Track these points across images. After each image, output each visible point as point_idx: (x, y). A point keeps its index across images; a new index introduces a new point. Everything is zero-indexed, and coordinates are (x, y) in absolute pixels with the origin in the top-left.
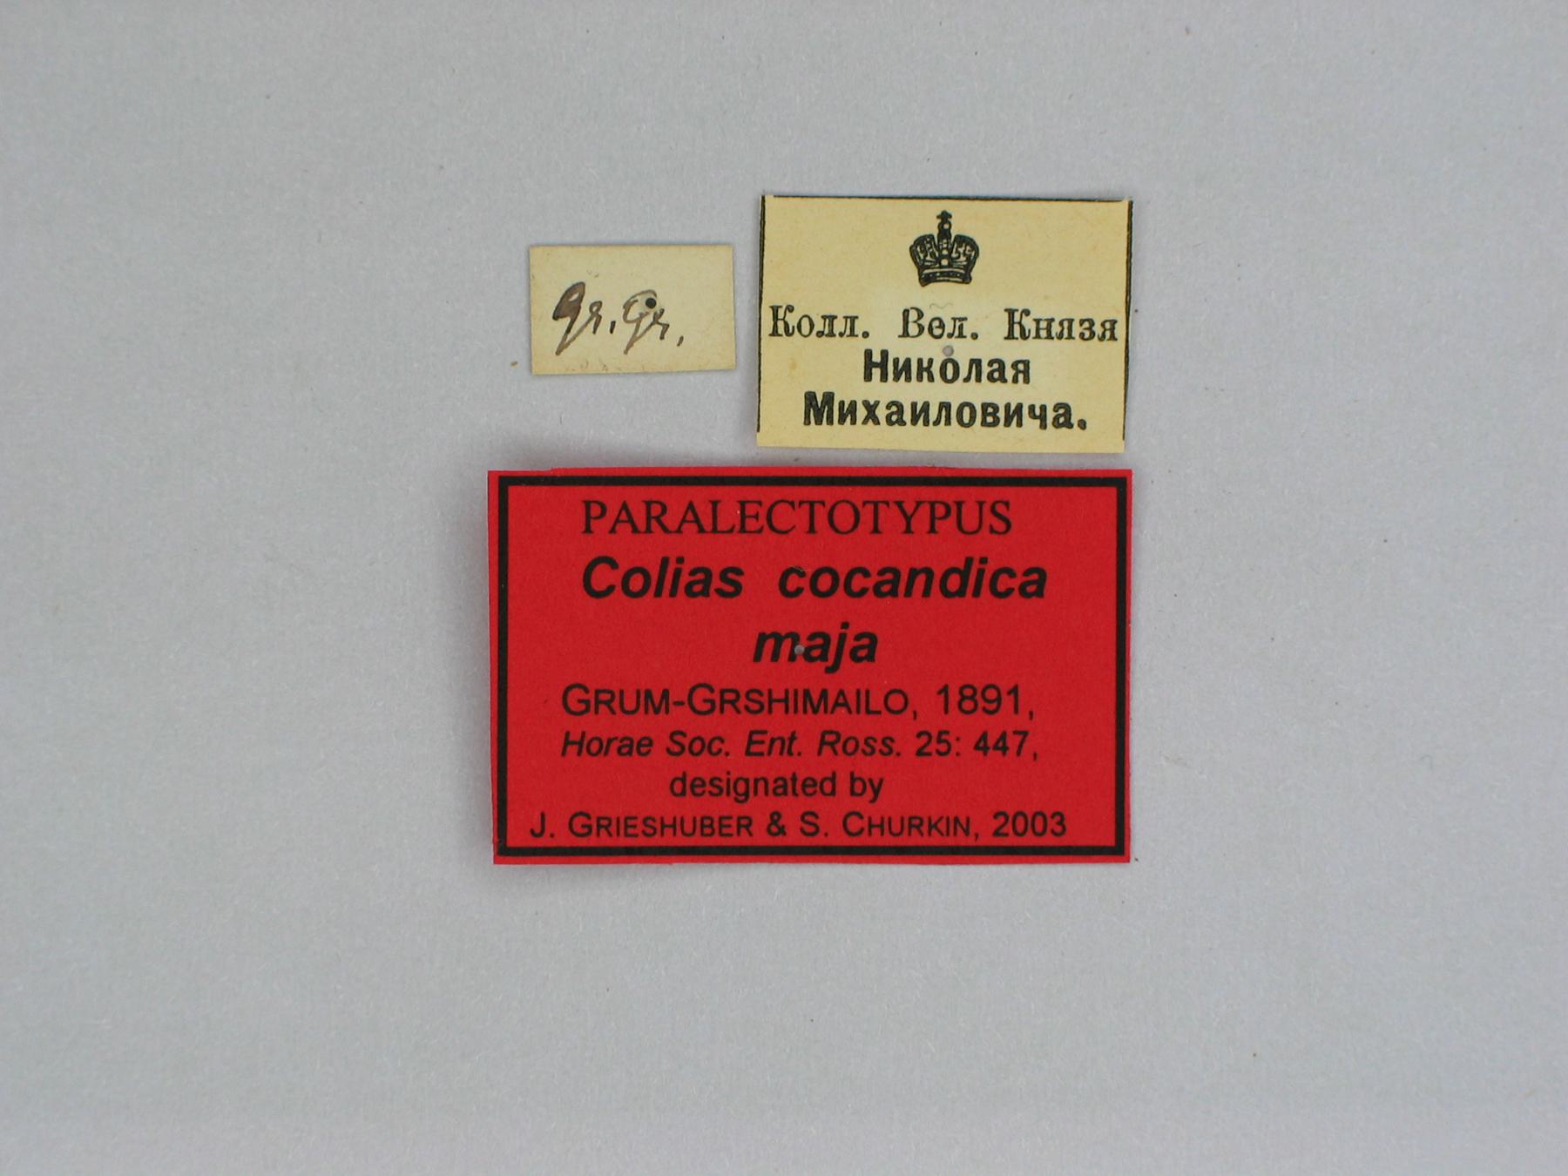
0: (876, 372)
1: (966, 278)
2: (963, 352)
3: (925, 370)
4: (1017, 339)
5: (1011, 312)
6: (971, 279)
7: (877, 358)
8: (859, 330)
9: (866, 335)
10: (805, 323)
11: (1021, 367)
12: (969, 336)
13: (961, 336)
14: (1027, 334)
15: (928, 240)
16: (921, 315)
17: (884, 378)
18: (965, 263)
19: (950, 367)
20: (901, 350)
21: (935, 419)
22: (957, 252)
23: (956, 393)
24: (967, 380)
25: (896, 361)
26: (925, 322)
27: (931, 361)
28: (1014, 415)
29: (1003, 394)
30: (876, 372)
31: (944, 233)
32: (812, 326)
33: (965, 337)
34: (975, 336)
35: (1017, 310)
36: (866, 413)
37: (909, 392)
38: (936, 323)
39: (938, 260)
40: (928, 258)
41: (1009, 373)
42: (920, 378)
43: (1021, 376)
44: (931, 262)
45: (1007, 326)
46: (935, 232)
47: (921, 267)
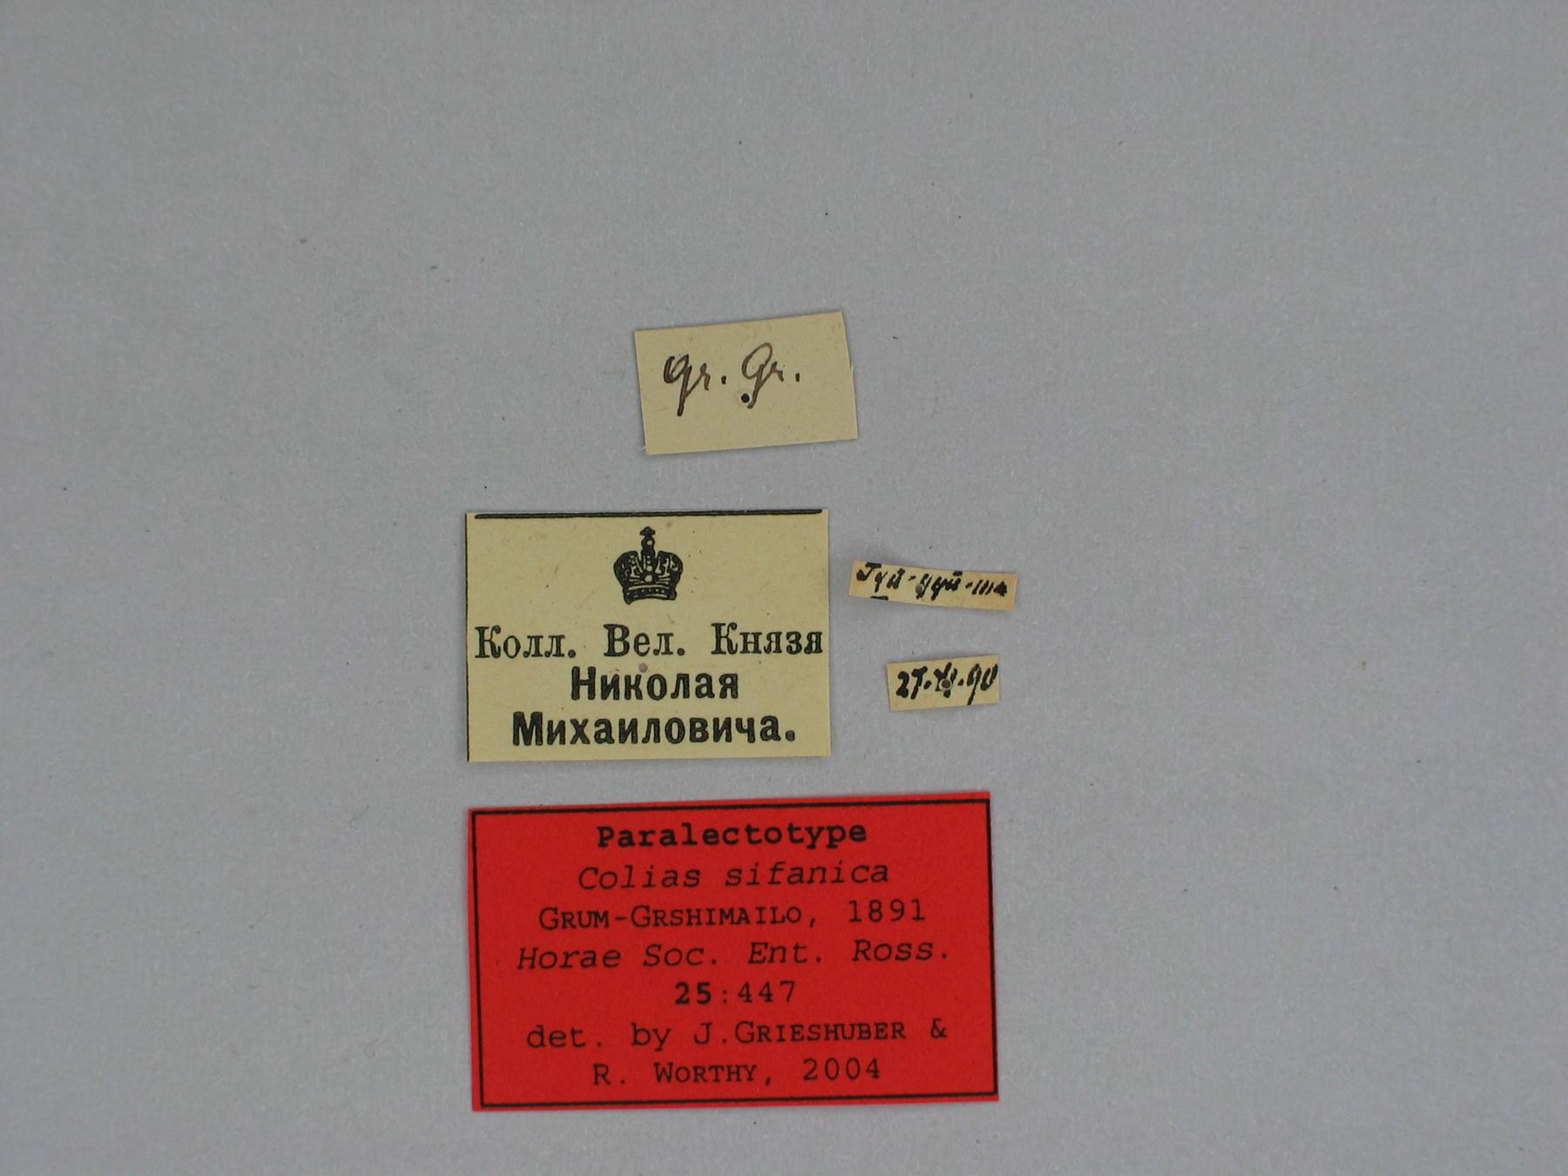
0: (584, 690)
1: (671, 593)
2: (669, 668)
3: (632, 687)
4: (725, 653)
5: (718, 627)
6: (676, 594)
7: (584, 676)
8: (564, 650)
9: (572, 654)
10: (512, 650)
11: (729, 681)
12: (675, 652)
13: (668, 652)
14: (734, 648)
15: (632, 557)
16: (626, 631)
17: (591, 695)
18: (668, 579)
19: (657, 684)
20: (608, 668)
21: (644, 736)
22: (662, 568)
23: (665, 710)
24: (675, 695)
25: (604, 678)
26: (631, 640)
27: (638, 678)
28: (723, 730)
29: (713, 709)
30: (584, 690)
31: (648, 549)
32: (518, 647)
33: (672, 653)
34: (681, 652)
35: (724, 624)
36: (585, 730)
37: (617, 710)
38: (642, 640)
39: (643, 577)
40: (633, 575)
41: (717, 688)
42: (628, 696)
43: (729, 691)
44: (634, 578)
45: (715, 640)
46: (639, 549)
47: (625, 582)
